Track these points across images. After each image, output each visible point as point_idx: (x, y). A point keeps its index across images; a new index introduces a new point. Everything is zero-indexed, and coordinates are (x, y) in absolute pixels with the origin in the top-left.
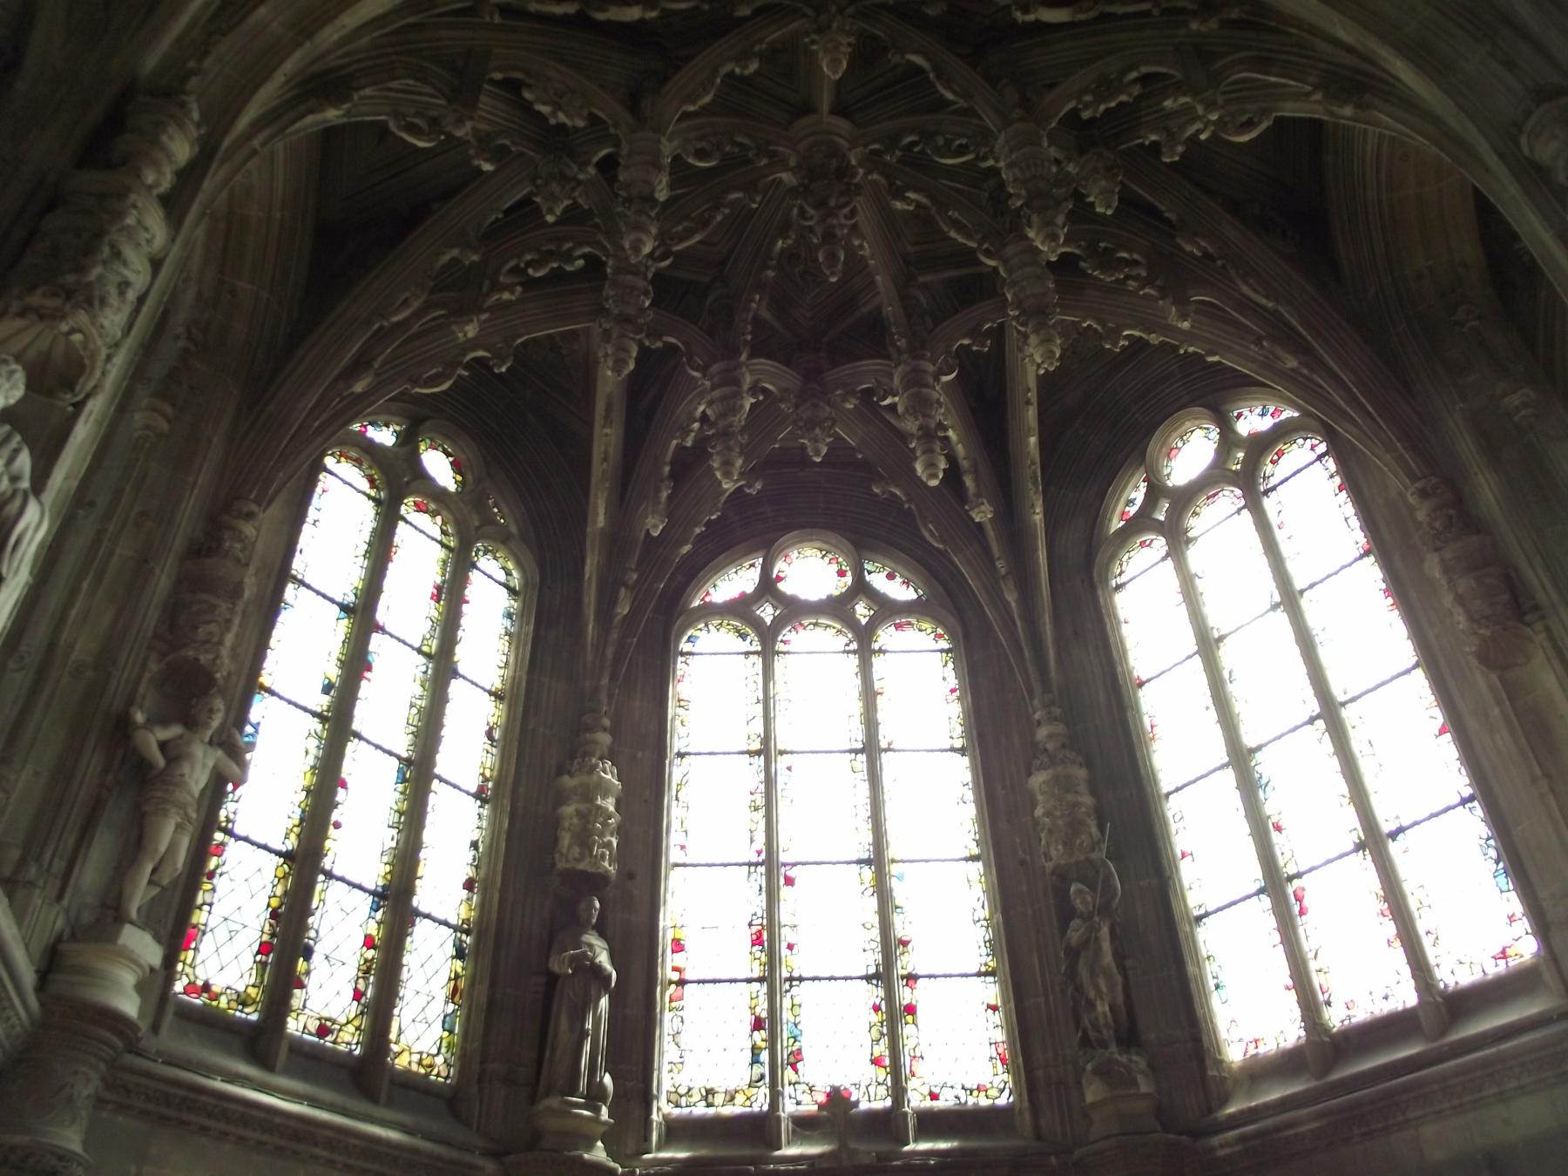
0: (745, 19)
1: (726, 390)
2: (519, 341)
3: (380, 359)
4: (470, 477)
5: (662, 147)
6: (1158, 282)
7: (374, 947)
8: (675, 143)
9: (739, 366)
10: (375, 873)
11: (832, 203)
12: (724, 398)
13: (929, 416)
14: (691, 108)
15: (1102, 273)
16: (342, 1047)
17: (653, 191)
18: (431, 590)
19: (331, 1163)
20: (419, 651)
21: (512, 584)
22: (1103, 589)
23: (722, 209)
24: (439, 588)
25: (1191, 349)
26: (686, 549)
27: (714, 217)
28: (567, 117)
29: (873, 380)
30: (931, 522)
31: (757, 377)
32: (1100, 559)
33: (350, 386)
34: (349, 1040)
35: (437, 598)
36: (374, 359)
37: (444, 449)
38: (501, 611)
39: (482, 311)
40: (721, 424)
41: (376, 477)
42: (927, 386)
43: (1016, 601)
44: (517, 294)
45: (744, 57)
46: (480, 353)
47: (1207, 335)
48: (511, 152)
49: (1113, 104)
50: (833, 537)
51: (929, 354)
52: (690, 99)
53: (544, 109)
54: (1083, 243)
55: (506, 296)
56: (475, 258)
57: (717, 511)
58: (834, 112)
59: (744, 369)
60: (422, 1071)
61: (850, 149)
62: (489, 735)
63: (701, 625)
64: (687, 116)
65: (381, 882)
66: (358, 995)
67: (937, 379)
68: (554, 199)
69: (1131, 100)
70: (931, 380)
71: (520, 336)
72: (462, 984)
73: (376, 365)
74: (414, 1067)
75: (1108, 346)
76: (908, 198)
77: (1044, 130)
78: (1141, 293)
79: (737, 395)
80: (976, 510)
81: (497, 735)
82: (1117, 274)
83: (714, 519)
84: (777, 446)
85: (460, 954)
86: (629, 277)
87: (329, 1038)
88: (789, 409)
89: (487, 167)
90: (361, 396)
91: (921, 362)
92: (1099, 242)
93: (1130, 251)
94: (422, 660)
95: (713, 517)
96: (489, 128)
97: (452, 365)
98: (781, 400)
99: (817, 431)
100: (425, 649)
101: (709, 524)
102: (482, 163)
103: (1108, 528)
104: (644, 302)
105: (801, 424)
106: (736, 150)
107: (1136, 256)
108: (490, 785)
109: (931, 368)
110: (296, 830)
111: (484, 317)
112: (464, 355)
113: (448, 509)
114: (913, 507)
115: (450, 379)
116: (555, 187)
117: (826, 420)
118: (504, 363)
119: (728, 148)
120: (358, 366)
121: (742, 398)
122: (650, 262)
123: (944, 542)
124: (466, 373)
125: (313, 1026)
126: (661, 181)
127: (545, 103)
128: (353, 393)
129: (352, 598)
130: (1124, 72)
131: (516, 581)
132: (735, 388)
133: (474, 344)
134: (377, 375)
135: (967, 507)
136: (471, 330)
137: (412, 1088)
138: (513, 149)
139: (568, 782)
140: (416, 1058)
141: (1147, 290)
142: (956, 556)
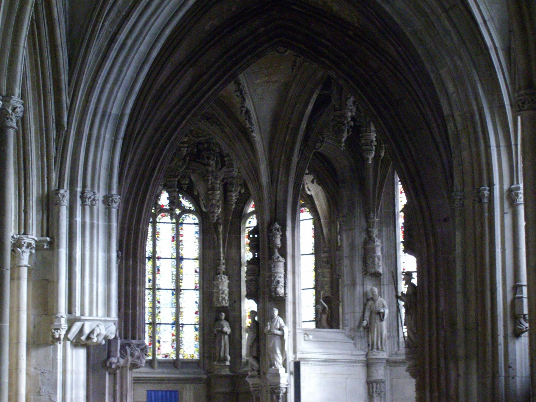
7: (174, 336)
10: (171, 319)
16: (171, 358)
18: (171, 238)
19: (169, 383)
20: (172, 258)
21: (196, 222)
24: (173, 237)
34: (173, 357)
35: (173, 241)
38: (194, 233)
60: (191, 358)
62: (196, 272)
63: (252, 217)
65: (173, 321)
66: (173, 347)
72: (198, 337)
74: (189, 358)
81: (198, 270)
85: (196, 330)
87: (168, 357)
94: (173, 260)
100: (173, 257)
108: (198, 285)
110: (151, 317)
125: (164, 356)
129: (151, 254)
131: (197, 221)
137: (189, 363)
139: (215, 283)
140: (189, 356)
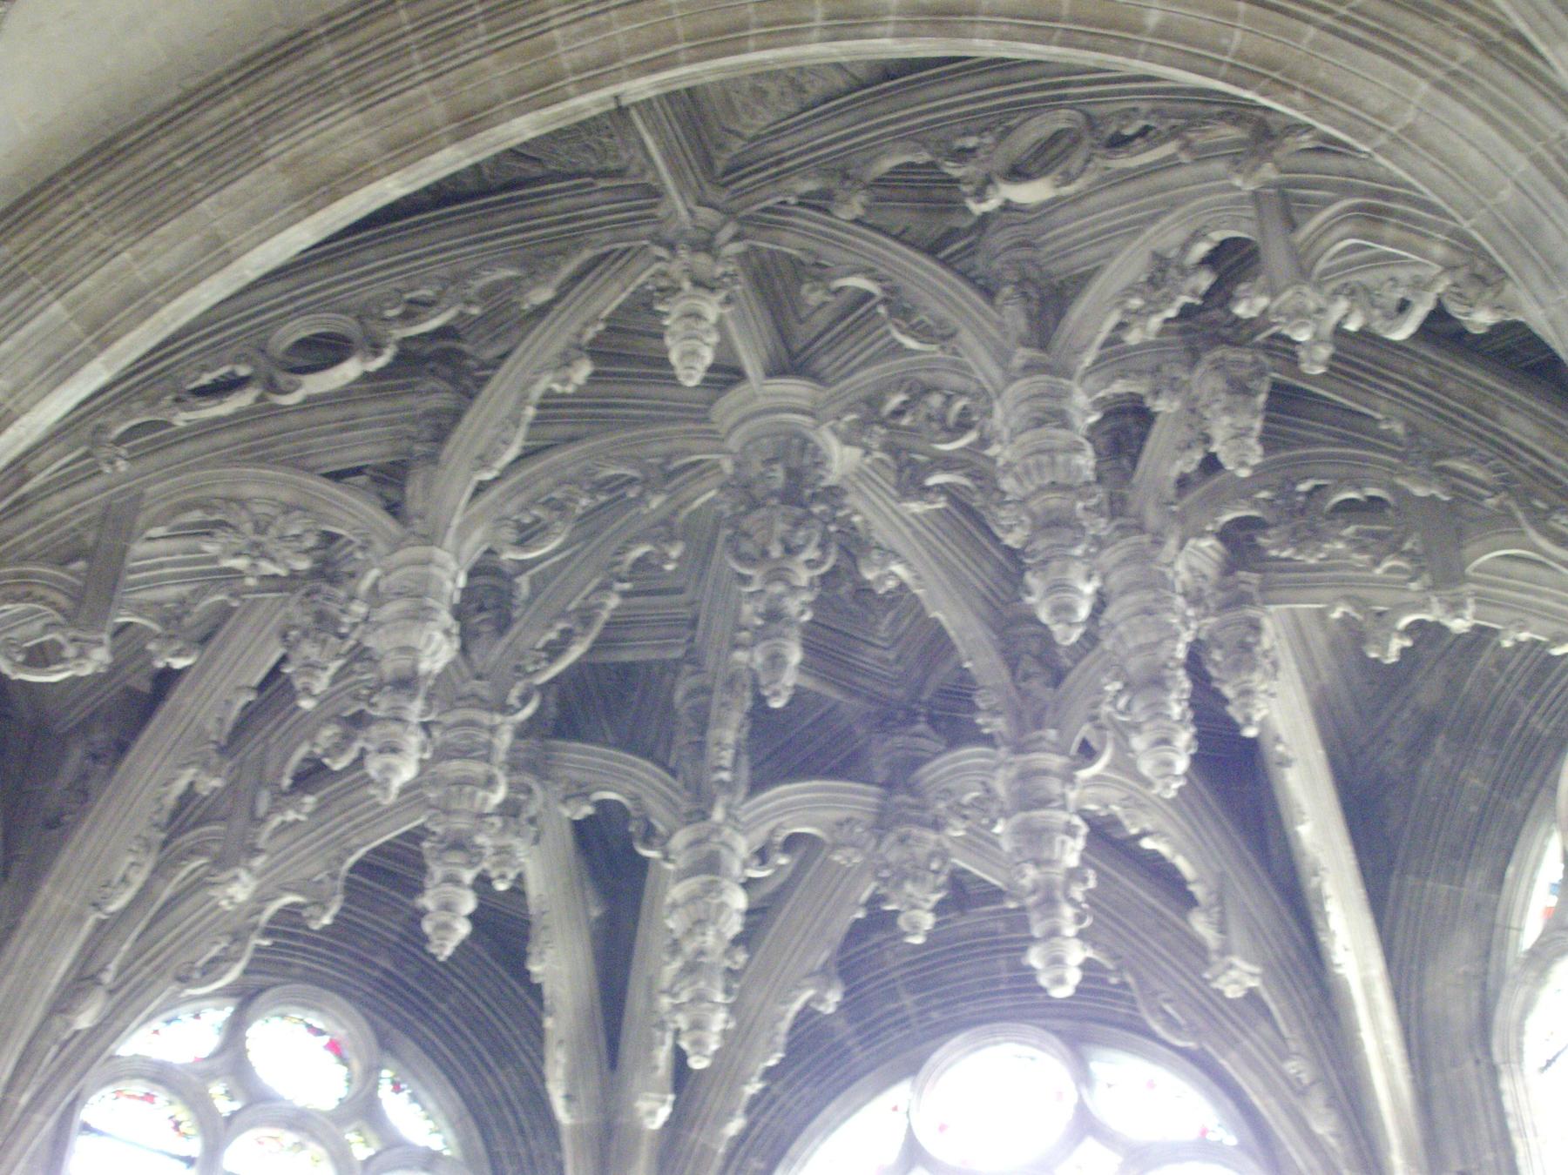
0: (542, 311)
1: (693, 884)
2: (352, 860)
3: (113, 967)
4: (356, 1065)
5: (435, 570)
6: (1407, 546)
8: (477, 535)
9: (716, 830)
11: (776, 551)
12: (692, 899)
13: (1049, 862)
14: (488, 476)
15: (1299, 551)
17: (416, 662)
22: (1512, 1076)
23: (619, 586)
25: (1524, 636)
26: (735, 1126)
27: (601, 606)
28: (273, 560)
29: (980, 787)
30: (1169, 1001)
31: (772, 824)
32: (1504, 1015)
33: (68, 1025)
36: (103, 969)
37: (310, 1027)
39: (255, 851)
40: (689, 947)
41: (179, 1118)
42: (1044, 803)
43: (1336, 1136)
44: (308, 809)
45: (566, 361)
46: (290, 899)
47: (1548, 602)
48: (234, 609)
49: (1171, 313)
50: (1027, 1028)
51: (1051, 734)
52: (484, 461)
53: (240, 563)
54: (1264, 494)
55: (291, 816)
56: (217, 783)
57: (775, 1051)
58: (776, 370)
59: (727, 831)
61: (816, 427)
64: (481, 488)
67: (1069, 779)
68: (311, 667)
69: (1198, 302)
70: (1054, 786)
71: (351, 852)
73: (107, 978)
75: (1373, 655)
76: (929, 489)
77: (1069, 376)
78: (1378, 571)
79: (711, 888)
80: (1223, 980)
82: (1327, 546)
83: (776, 1067)
84: (860, 914)
86: (455, 765)
88: (849, 859)
89: (179, 663)
90: (94, 1032)
91: (1034, 756)
92: (1294, 484)
93: (1358, 487)
95: (772, 1062)
96: (185, 590)
97: (238, 937)
98: (836, 846)
99: (909, 887)
101: (769, 1074)
102: (170, 660)
103: (1517, 945)
104: (485, 800)
105: (885, 873)
106: (603, 498)
107: (1373, 492)
109: (1056, 761)
111: (259, 862)
112: (260, 912)
113: (314, 1137)
114: (1129, 979)
115: (237, 960)
116: (309, 650)
117: (932, 856)
118: (325, 909)
119: (584, 502)
120: (81, 982)
121: (721, 892)
122: (498, 718)
123: (1196, 1034)
124: (266, 943)
126: (430, 639)
127: (237, 555)
128: (77, 1033)
130: (1185, 247)
132: (704, 878)
133: (261, 899)
134: (112, 992)
135: (1207, 975)
136: (240, 890)
138: (235, 603)
141: (1389, 563)
142: (1224, 1056)
